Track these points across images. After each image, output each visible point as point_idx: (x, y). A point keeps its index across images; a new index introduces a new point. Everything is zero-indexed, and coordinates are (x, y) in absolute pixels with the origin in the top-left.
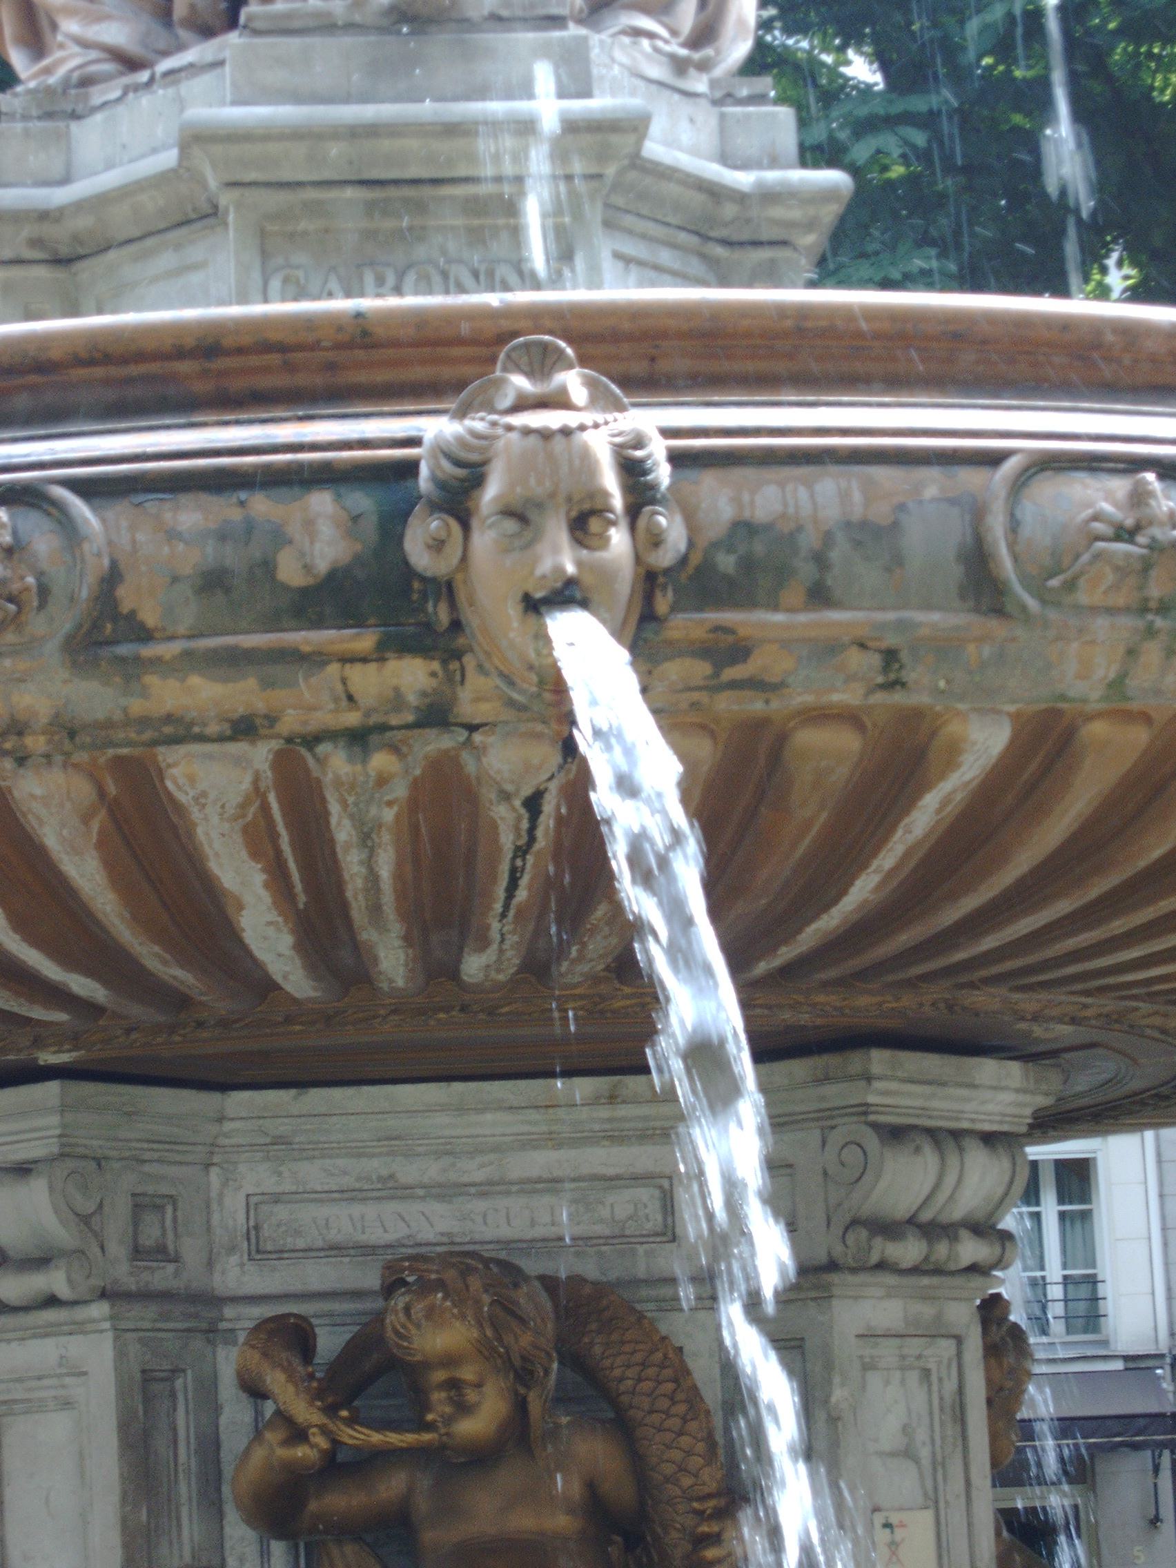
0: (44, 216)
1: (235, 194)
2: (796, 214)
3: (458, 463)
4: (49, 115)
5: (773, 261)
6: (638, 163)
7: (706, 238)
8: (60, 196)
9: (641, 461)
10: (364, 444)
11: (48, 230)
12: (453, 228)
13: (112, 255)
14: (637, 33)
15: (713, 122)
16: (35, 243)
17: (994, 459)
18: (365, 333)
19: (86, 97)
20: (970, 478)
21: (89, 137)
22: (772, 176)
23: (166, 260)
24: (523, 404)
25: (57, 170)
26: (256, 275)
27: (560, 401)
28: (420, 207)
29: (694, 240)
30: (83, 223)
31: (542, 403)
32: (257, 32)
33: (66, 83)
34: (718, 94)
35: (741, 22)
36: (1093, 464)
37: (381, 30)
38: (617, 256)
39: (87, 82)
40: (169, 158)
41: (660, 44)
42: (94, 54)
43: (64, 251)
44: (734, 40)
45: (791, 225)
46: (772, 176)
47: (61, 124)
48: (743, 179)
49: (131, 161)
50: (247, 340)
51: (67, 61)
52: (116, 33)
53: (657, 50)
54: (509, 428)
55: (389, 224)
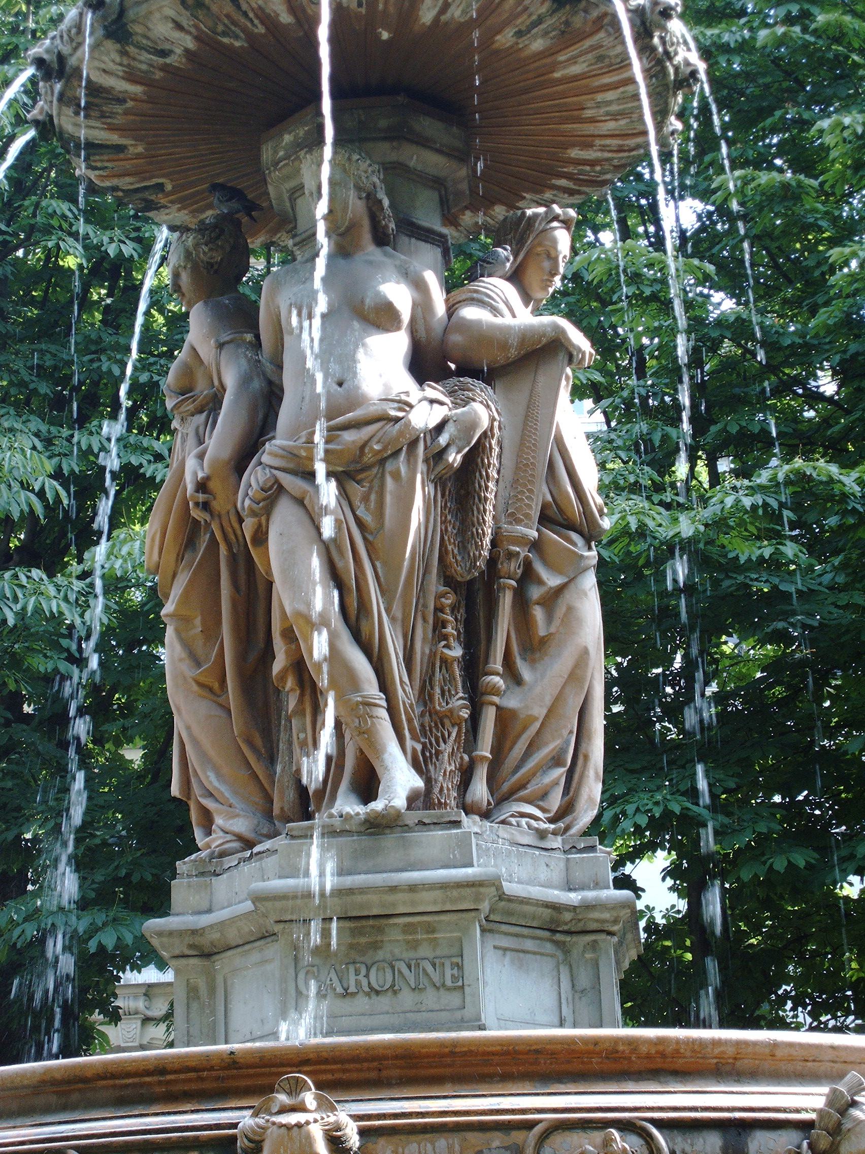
0: (194, 932)
1: (281, 926)
2: (606, 915)
3: (250, 1140)
4: (202, 874)
5: (595, 941)
6: (502, 896)
7: (554, 932)
8: (205, 920)
9: (340, 1137)
10: (218, 1127)
11: (198, 940)
12: (398, 941)
13: (229, 953)
14: (523, 815)
15: (562, 865)
16: (191, 946)
17: (529, 1125)
18: (235, 1062)
19: (222, 864)
20: (517, 1136)
21: (220, 885)
22: (591, 894)
23: (255, 957)
24: (283, 1110)
25: (205, 905)
26: (292, 971)
27: (300, 1108)
28: (380, 930)
29: (547, 934)
30: (216, 936)
31: (294, 1109)
32: (293, 837)
33: (212, 856)
34: (567, 847)
35: (591, 799)
36: (585, 1125)
37: (359, 833)
38: (495, 947)
39: (223, 854)
40: (248, 906)
41: (533, 822)
42: (229, 837)
43: (206, 951)
44: (586, 811)
45: (604, 921)
46: (591, 894)
47: (208, 879)
48: (574, 898)
49: (239, 902)
50: (176, 1066)
51: (217, 840)
52: (242, 825)
53: (529, 827)
54: (274, 1123)
55: (363, 940)
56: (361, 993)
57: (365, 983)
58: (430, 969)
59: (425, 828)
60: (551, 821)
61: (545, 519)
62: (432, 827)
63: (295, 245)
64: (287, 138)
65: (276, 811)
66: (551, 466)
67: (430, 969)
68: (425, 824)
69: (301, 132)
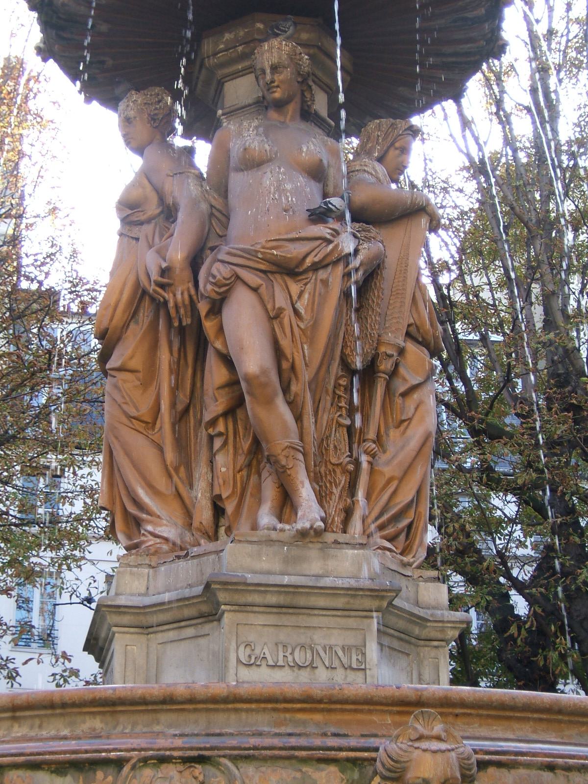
56: (287, 668)
57: (290, 659)
58: (340, 653)
59: (338, 546)
60: (401, 554)
61: (408, 335)
62: (345, 546)
63: (223, 115)
64: (227, 36)
65: (196, 524)
66: (414, 299)
67: (340, 653)
68: (339, 543)
69: (242, 33)
